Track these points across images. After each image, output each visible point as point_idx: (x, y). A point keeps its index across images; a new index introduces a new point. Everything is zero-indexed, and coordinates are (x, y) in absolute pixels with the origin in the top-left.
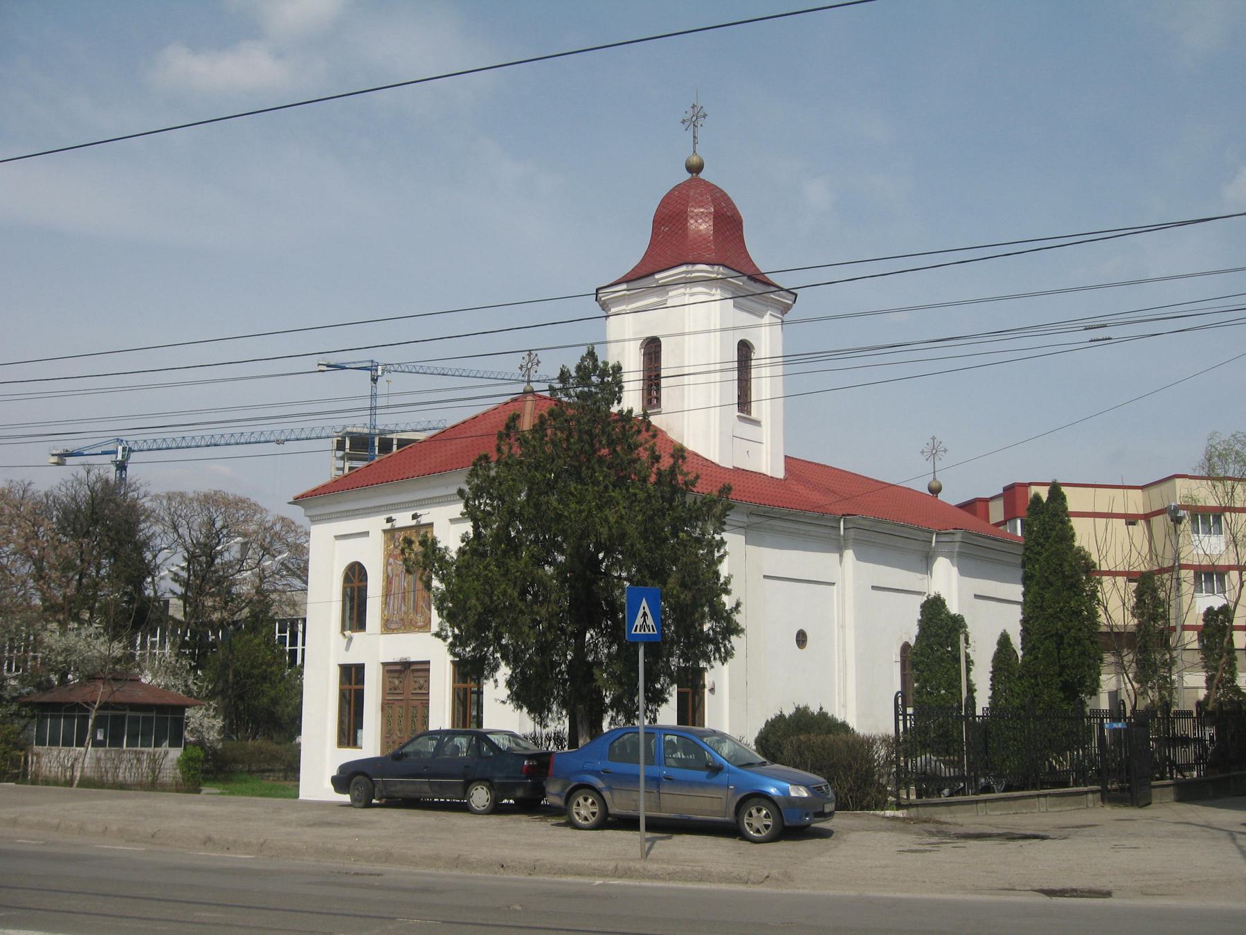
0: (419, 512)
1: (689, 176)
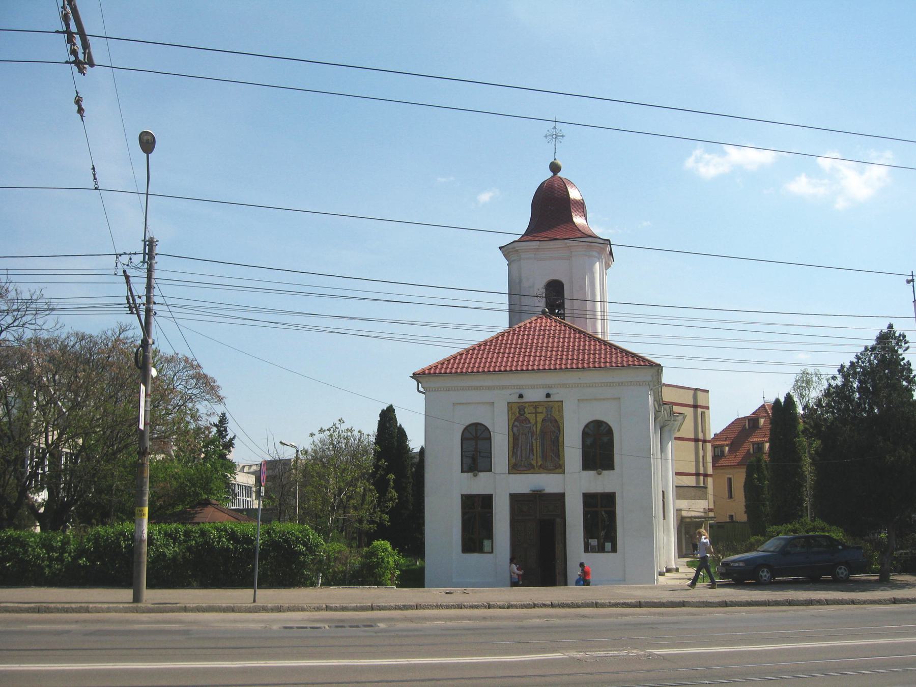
0: (550, 391)
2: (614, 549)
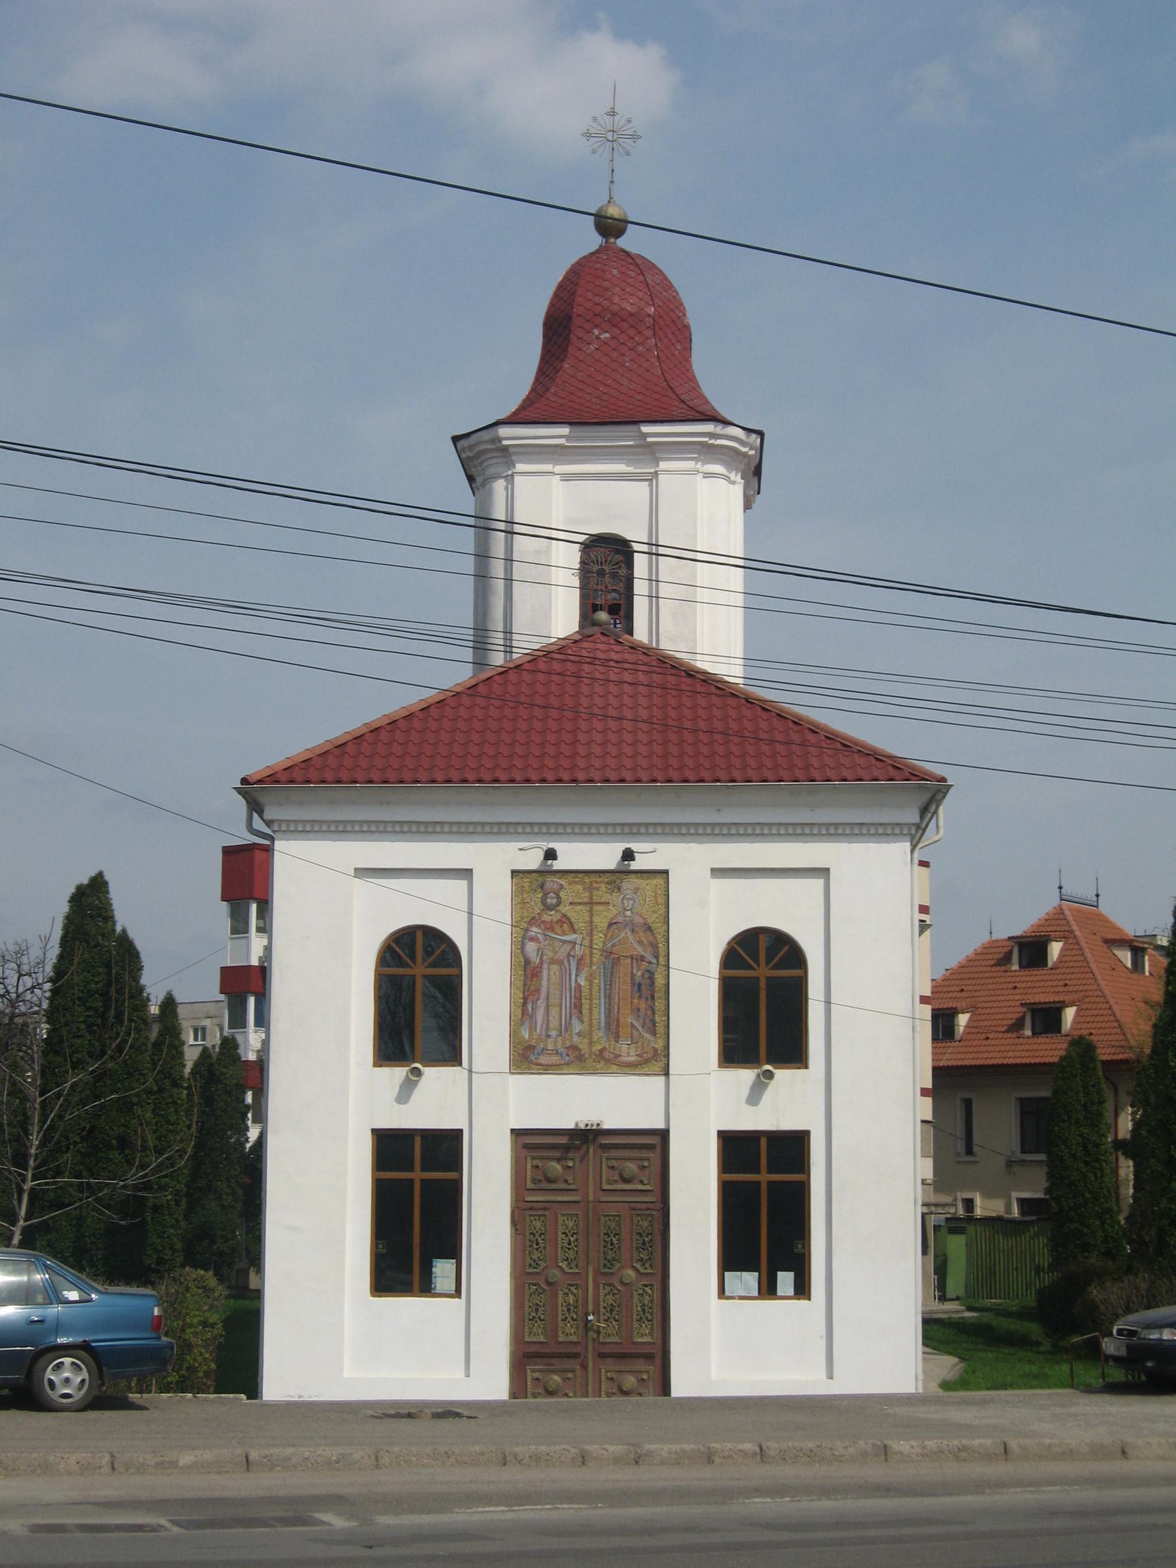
2: (802, 1289)
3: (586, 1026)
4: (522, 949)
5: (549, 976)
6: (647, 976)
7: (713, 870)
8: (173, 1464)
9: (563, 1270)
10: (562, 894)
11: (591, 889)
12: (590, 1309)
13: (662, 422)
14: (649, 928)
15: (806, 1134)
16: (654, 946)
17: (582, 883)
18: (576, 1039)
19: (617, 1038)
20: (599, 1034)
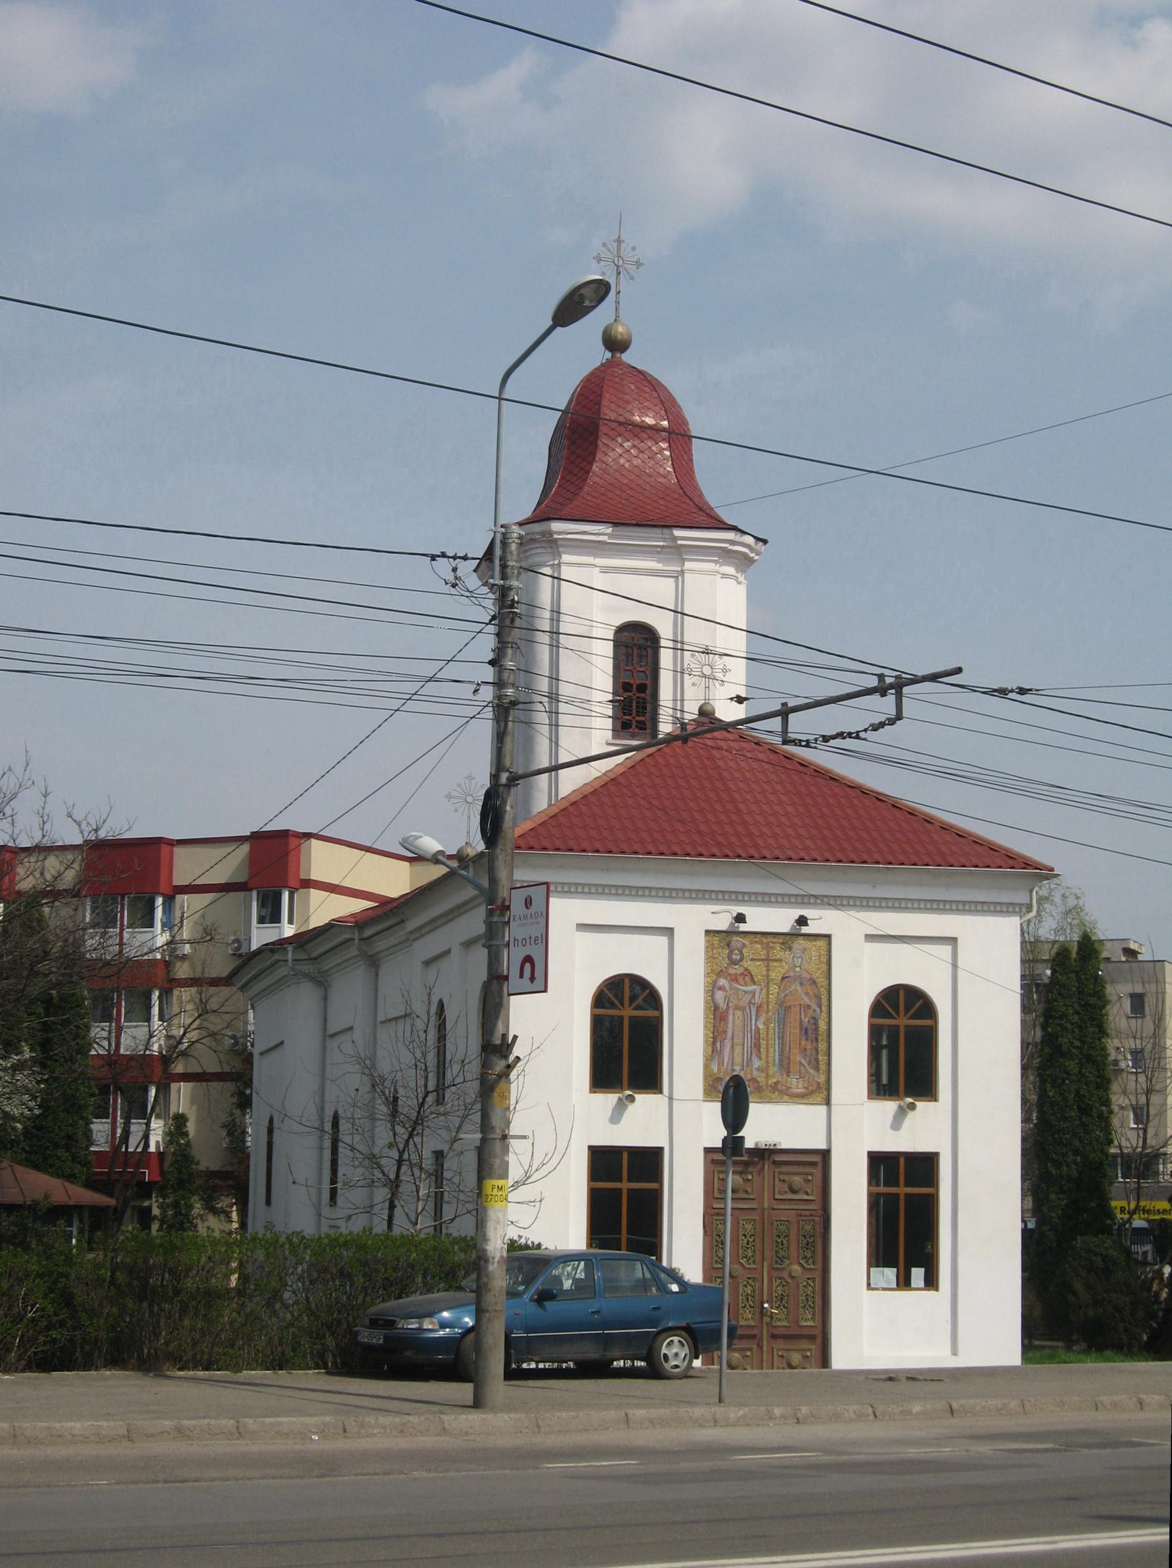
1: (608, 355)
2: (931, 1282)
3: (763, 1062)
4: (713, 996)
5: (734, 1020)
6: (812, 1021)
7: (866, 935)
8: (909, 1412)
9: (802, 1266)
10: (744, 951)
11: (768, 948)
12: (765, 1299)
13: (691, 528)
14: (814, 982)
15: (936, 1154)
16: (818, 997)
17: (761, 943)
18: (755, 1073)
19: (788, 1073)
20: (773, 1069)
